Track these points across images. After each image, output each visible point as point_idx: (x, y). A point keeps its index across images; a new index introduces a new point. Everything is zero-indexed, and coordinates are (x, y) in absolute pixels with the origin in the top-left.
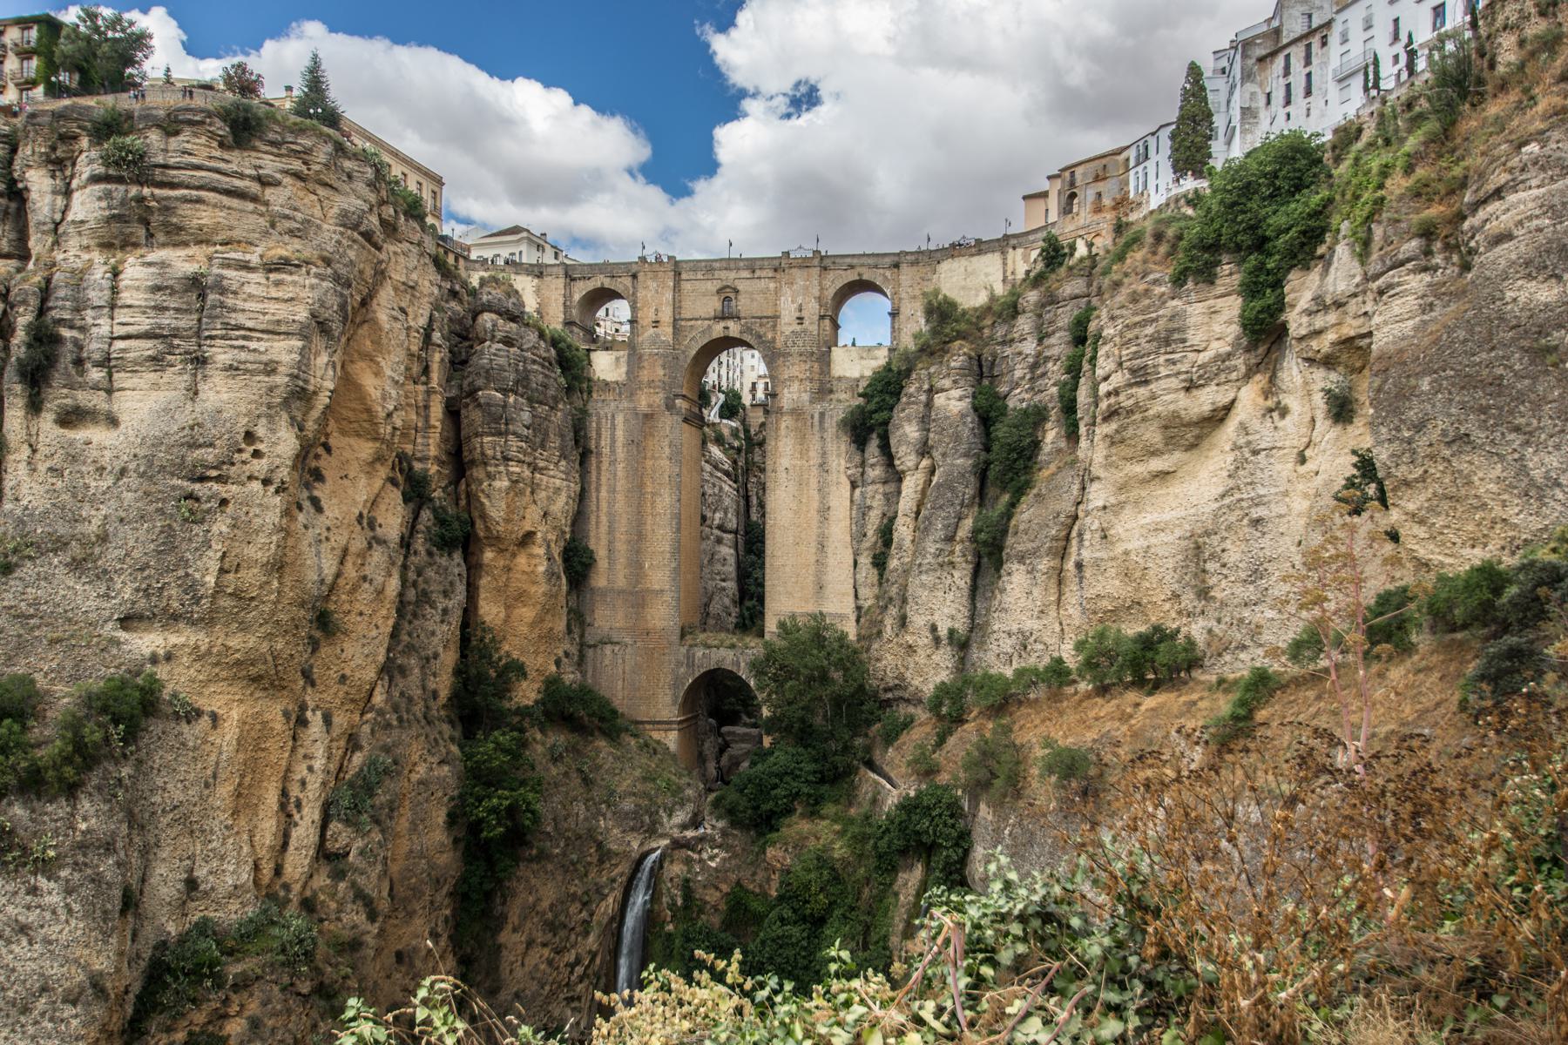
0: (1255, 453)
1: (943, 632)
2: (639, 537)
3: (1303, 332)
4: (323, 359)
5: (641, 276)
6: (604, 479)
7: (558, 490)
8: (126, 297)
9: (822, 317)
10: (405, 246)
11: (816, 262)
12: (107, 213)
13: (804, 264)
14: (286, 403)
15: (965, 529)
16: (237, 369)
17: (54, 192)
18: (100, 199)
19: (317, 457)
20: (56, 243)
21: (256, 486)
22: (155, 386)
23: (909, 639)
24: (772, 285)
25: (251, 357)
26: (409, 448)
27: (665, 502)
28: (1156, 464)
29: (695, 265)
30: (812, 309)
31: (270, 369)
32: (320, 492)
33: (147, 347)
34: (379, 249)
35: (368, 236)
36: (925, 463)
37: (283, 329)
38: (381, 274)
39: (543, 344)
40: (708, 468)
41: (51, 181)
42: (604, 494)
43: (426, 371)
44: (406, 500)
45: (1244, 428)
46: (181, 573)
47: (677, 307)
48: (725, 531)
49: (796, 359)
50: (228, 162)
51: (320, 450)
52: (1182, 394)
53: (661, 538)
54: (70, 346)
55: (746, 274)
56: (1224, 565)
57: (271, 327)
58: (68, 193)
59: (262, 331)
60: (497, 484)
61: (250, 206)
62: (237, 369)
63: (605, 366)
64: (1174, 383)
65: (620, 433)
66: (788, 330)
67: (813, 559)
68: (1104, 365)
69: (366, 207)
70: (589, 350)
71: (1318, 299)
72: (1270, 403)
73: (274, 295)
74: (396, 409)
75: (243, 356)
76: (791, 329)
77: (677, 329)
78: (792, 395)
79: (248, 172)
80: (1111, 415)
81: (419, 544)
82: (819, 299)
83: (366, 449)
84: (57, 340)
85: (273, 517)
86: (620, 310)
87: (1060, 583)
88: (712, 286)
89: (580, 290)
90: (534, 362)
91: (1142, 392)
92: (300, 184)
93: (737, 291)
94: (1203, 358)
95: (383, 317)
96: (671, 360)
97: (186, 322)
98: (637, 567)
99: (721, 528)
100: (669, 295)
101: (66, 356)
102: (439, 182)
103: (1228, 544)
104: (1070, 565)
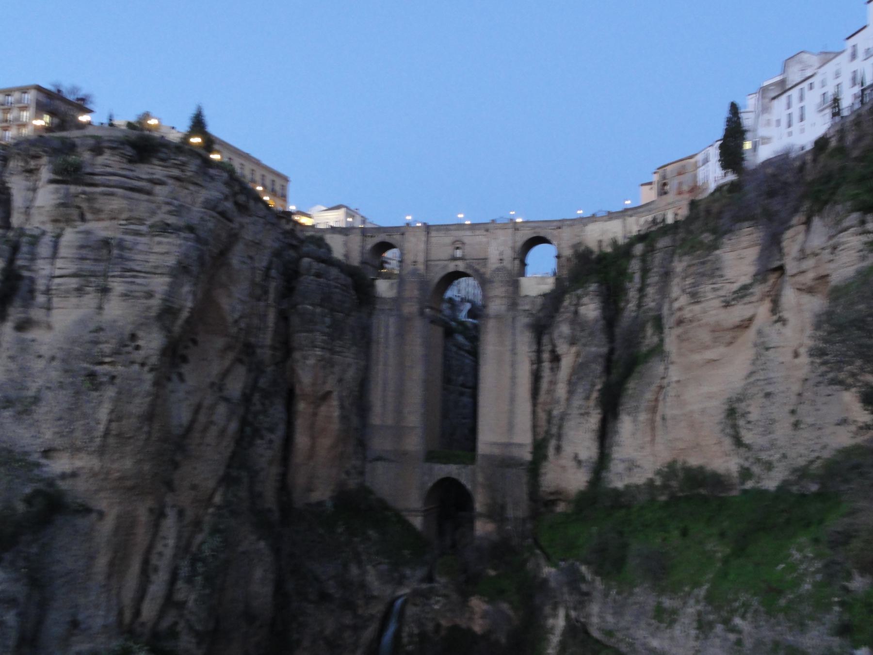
0: (767, 349)
2: (401, 393)
3: (794, 271)
4: (186, 289)
7: (349, 365)
8: (63, 251)
9: (514, 259)
10: (255, 218)
11: (511, 225)
13: (504, 227)
14: (160, 317)
15: (595, 395)
16: (129, 296)
17: (29, 189)
18: (53, 193)
19: (186, 347)
20: (27, 220)
21: (136, 367)
22: (78, 307)
23: (563, 462)
24: (484, 239)
26: (253, 340)
27: (417, 373)
28: (709, 355)
30: (508, 254)
31: (150, 295)
32: (185, 369)
33: (74, 283)
34: (230, 220)
35: (223, 214)
36: (574, 349)
37: (159, 271)
38: (234, 237)
39: (342, 276)
40: (454, 349)
41: (24, 183)
42: (381, 367)
43: (266, 292)
44: (250, 370)
45: (760, 333)
47: (427, 252)
48: (466, 387)
50: (132, 170)
51: (190, 344)
52: (723, 311)
53: (415, 394)
54: (27, 282)
55: (468, 233)
56: (749, 422)
57: (153, 270)
58: (34, 190)
59: (145, 272)
61: (145, 197)
62: (129, 296)
63: (383, 287)
64: (717, 303)
65: (392, 330)
66: (494, 266)
68: (675, 291)
69: (222, 196)
70: (374, 279)
71: (802, 250)
72: (775, 318)
73: (157, 249)
74: (241, 317)
75: (134, 287)
77: (427, 267)
78: (496, 306)
79: (144, 176)
80: (680, 322)
81: (256, 398)
82: (513, 248)
83: (220, 342)
84: (20, 278)
85: (147, 386)
86: (389, 254)
87: (653, 429)
88: (448, 240)
89: (371, 243)
90: (336, 287)
91: (697, 308)
92: (178, 183)
93: (463, 243)
94: (735, 287)
95: (235, 260)
96: (423, 284)
97: (100, 267)
98: (399, 411)
99: (463, 385)
100: (422, 246)
101: (24, 286)
102: (286, 179)
103: (750, 409)
104: (658, 418)
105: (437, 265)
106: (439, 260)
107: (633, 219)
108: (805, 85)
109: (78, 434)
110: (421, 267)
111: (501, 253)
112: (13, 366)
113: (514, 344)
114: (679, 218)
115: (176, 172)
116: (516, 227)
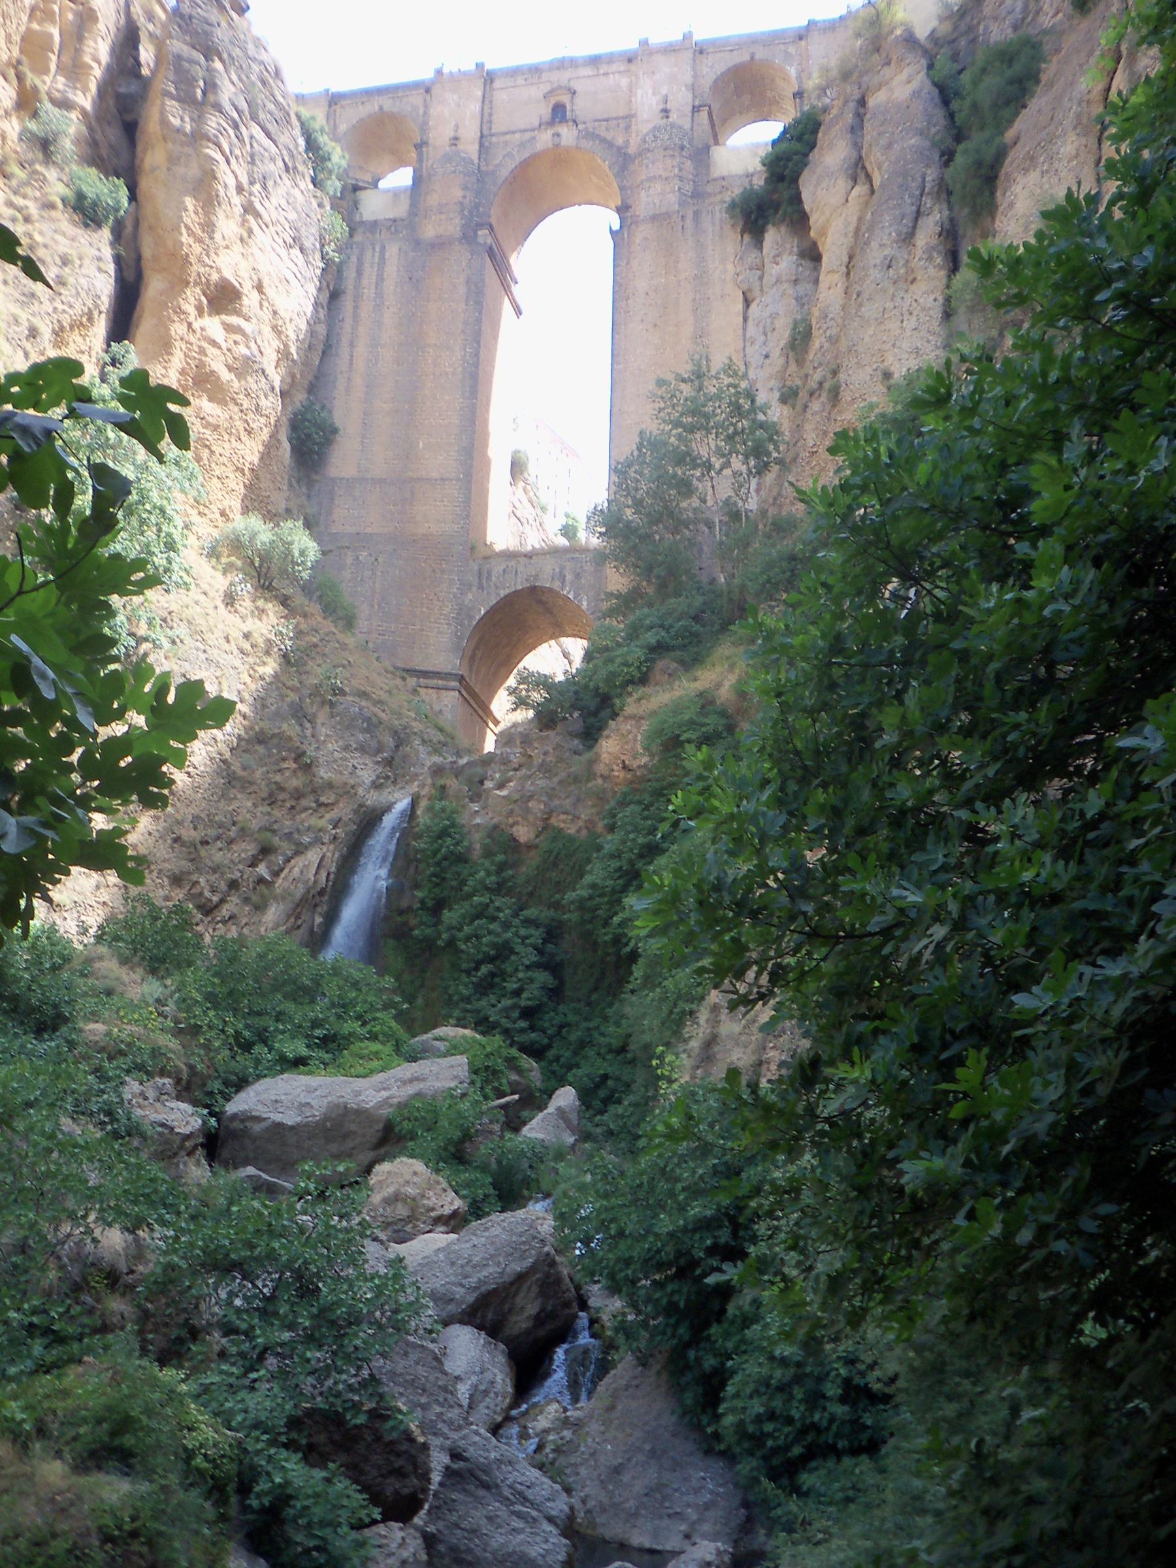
5: (435, 90)
6: (362, 330)
9: (696, 109)
13: (670, 50)
24: (624, 82)
29: (513, 73)
30: (681, 100)
42: (361, 350)
47: (486, 120)
55: (588, 71)
65: (392, 269)
66: (645, 128)
76: (651, 126)
82: (693, 88)
88: (537, 92)
100: (475, 107)
105: (506, 143)
106: (513, 132)
110: (470, 149)
116: (701, 50)
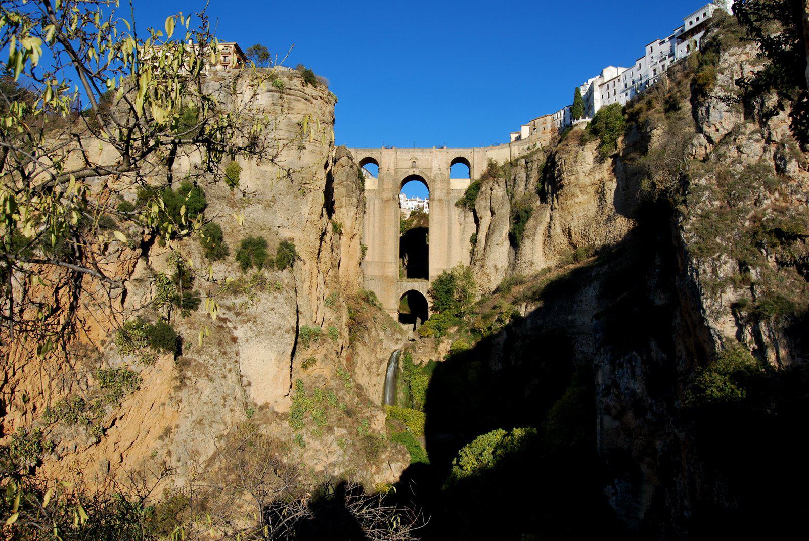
1: (499, 266)
12: (271, 102)
24: (430, 158)
25: (316, 149)
46: (299, 213)
47: (396, 164)
49: (439, 182)
55: (420, 153)
60: (349, 214)
65: (377, 206)
67: (447, 250)
77: (396, 172)
88: (409, 157)
100: (393, 160)
107: (516, 147)
108: (616, 80)
109: (296, 218)
110: (393, 172)
111: (440, 165)
112: (259, 183)
113: (450, 215)
114: (543, 146)
115: (321, 95)
